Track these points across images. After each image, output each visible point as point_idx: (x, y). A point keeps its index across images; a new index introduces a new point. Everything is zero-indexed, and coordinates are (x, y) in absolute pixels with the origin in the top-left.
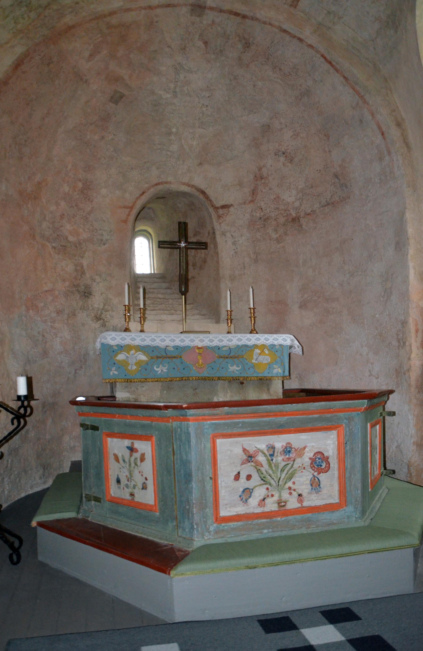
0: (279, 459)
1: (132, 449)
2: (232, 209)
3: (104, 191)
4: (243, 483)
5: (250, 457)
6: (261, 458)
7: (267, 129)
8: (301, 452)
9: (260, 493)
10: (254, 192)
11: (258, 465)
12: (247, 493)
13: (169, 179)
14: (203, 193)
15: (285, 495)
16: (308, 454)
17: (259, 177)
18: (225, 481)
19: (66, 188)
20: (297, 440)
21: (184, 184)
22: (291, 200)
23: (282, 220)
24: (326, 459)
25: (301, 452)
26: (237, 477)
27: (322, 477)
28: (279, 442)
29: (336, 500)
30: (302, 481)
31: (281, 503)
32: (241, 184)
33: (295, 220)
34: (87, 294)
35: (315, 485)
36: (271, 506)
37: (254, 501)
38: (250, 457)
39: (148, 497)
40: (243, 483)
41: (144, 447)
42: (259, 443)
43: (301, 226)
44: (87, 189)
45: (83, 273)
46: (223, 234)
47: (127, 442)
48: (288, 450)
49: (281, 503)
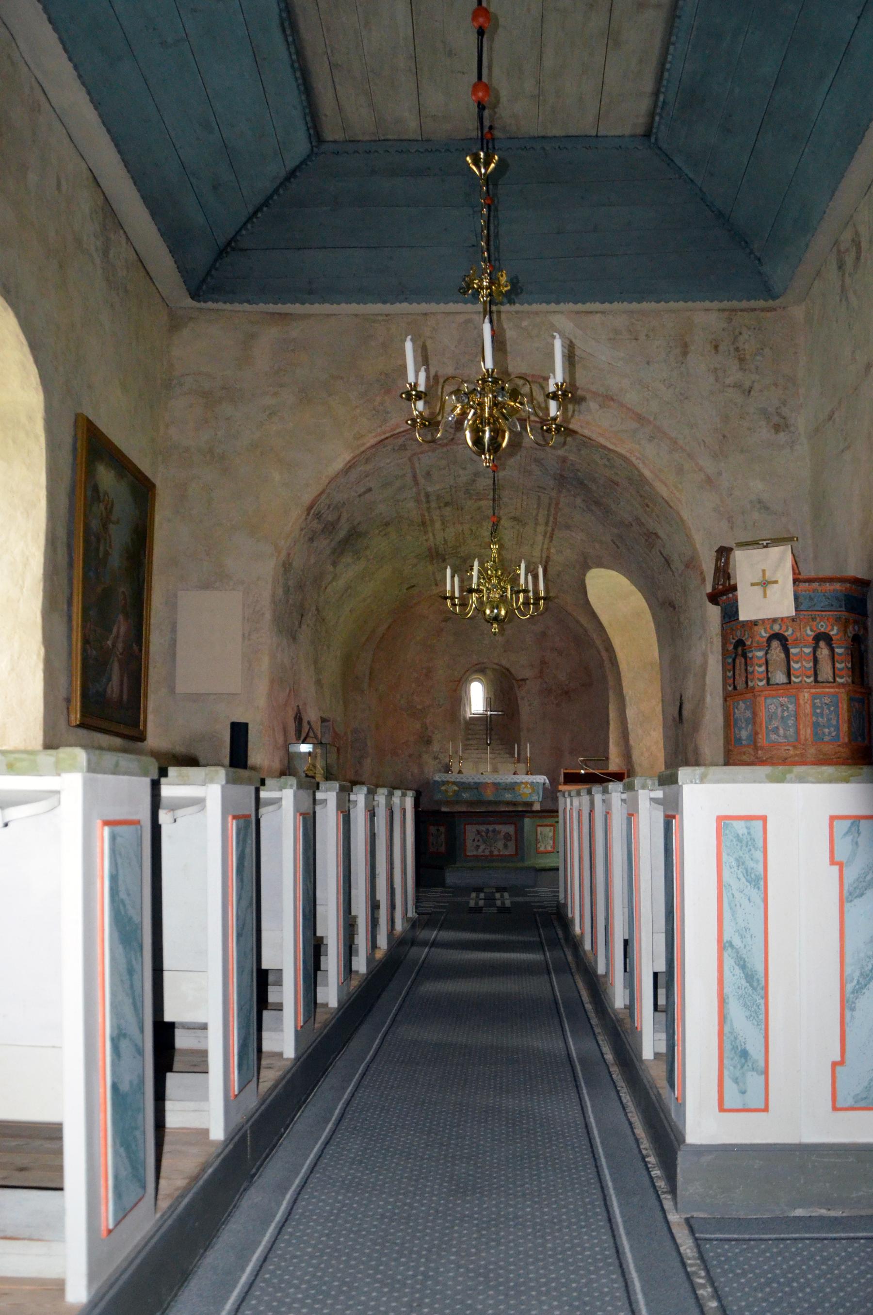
0: (490, 834)
1: (438, 830)
2: (528, 682)
3: (440, 672)
4: (476, 843)
5: (478, 832)
6: (483, 834)
7: (544, 634)
8: (499, 832)
9: (482, 847)
10: (541, 672)
11: (482, 836)
12: (478, 847)
13: (485, 660)
14: (508, 670)
15: (493, 849)
16: (503, 834)
17: (543, 662)
18: (469, 843)
19: (416, 675)
20: (498, 827)
21: (496, 664)
22: (563, 679)
23: (559, 692)
24: (510, 835)
25: (499, 832)
26: (474, 840)
27: (509, 844)
28: (491, 828)
29: (513, 853)
30: (500, 844)
31: (491, 852)
32: (532, 666)
33: (567, 693)
34: (429, 742)
35: (506, 846)
36: (487, 853)
37: (480, 850)
38: (478, 832)
39: (443, 849)
40: (476, 843)
41: (442, 829)
42: (483, 828)
43: (570, 697)
44: (429, 673)
45: (427, 728)
46: (523, 698)
47: (436, 828)
48: (494, 831)
49: (491, 852)
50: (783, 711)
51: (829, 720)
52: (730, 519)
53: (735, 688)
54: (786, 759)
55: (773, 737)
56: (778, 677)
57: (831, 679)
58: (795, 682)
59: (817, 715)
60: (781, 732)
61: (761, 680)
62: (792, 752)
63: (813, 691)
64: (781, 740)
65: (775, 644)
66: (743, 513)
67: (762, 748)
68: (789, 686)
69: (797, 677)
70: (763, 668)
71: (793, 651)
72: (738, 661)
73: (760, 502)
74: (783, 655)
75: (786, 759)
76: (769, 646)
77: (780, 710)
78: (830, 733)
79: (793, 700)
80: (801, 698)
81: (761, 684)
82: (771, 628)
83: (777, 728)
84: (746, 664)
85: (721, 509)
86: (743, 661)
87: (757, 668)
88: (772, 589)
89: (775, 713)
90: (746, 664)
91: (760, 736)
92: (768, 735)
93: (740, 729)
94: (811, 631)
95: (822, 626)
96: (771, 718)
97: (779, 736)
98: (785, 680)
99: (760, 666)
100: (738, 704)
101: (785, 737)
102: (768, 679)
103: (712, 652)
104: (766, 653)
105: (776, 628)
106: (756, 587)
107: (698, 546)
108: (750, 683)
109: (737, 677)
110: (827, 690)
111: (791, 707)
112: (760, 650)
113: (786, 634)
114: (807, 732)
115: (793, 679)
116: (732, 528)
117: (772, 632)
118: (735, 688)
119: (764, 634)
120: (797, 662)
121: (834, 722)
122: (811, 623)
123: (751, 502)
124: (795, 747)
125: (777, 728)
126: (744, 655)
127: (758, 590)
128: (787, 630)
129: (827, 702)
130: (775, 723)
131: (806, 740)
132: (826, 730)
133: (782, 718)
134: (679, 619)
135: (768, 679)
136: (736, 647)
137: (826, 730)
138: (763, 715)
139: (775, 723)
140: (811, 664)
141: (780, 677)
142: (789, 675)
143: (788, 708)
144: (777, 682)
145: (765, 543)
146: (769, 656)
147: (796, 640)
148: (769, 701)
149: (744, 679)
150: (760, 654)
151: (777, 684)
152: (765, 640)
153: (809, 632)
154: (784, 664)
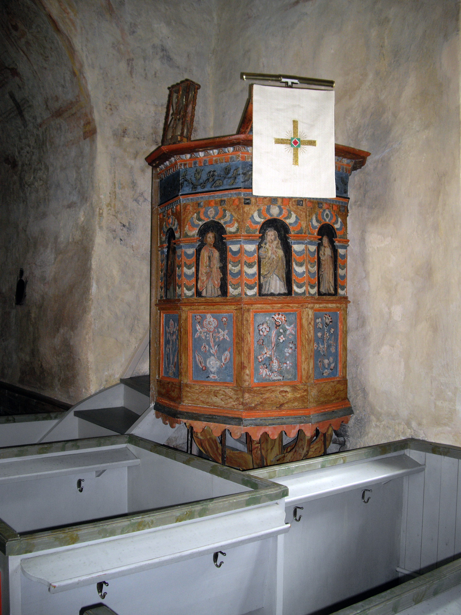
50: (279, 335)
51: (329, 346)
52: (130, 61)
53: (198, 293)
54: (282, 405)
55: (264, 372)
56: (273, 283)
57: (332, 291)
58: (297, 294)
59: (318, 341)
60: (275, 365)
61: (251, 288)
62: (290, 395)
63: (317, 306)
64: (275, 377)
65: (271, 234)
66: (145, 59)
67: (250, 390)
68: (289, 298)
69: (300, 287)
70: (255, 269)
71: (296, 248)
72: (205, 254)
73: (163, 50)
74: (281, 253)
75: (282, 405)
76: (263, 238)
77: (274, 332)
78: (329, 364)
79: (292, 318)
80: (304, 316)
81: (250, 293)
82: (268, 210)
83: (270, 359)
84: (223, 259)
85: (122, 47)
86: (216, 254)
87: (246, 269)
88: (305, 152)
89: (268, 336)
90: (223, 259)
91: (247, 372)
92: (257, 370)
93: (207, 354)
94: (317, 221)
95: (327, 215)
96: (261, 345)
97: (271, 370)
98: (283, 290)
99: (250, 266)
100: (203, 318)
101: (280, 373)
102: (260, 287)
103: (101, 228)
104: (259, 247)
105: (275, 211)
106: (282, 146)
107: (90, 88)
108: (230, 290)
109: (203, 277)
110: (330, 305)
111: (290, 329)
112: (250, 242)
113: (288, 221)
114: (307, 366)
115: (295, 288)
116: (131, 73)
117: (269, 217)
118: (198, 293)
119: (257, 219)
120: (301, 265)
121: (333, 350)
122: (317, 210)
123: (154, 47)
124: (295, 388)
125: (270, 359)
126: (221, 246)
127: (286, 151)
128: (289, 217)
129: (328, 321)
130: (267, 352)
131: (308, 377)
132: (326, 361)
133: (277, 344)
134: (21, 179)
135: (260, 287)
136: (203, 232)
137: (326, 361)
138: (251, 339)
139: (267, 352)
140: (316, 268)
141: (276, 285)
142: (289, 282)
143: (285, 330)
144: (272, 291)
145: (290, 81)
146: (262, 251)
147: (300, 232)
148: (260, 318)
149: (217, 282)
150: (251, 247)
151: (272, 294)
152: (258, 227)
153: (315, 223)
154: (282, 264)
